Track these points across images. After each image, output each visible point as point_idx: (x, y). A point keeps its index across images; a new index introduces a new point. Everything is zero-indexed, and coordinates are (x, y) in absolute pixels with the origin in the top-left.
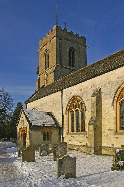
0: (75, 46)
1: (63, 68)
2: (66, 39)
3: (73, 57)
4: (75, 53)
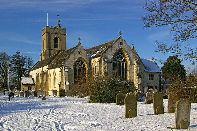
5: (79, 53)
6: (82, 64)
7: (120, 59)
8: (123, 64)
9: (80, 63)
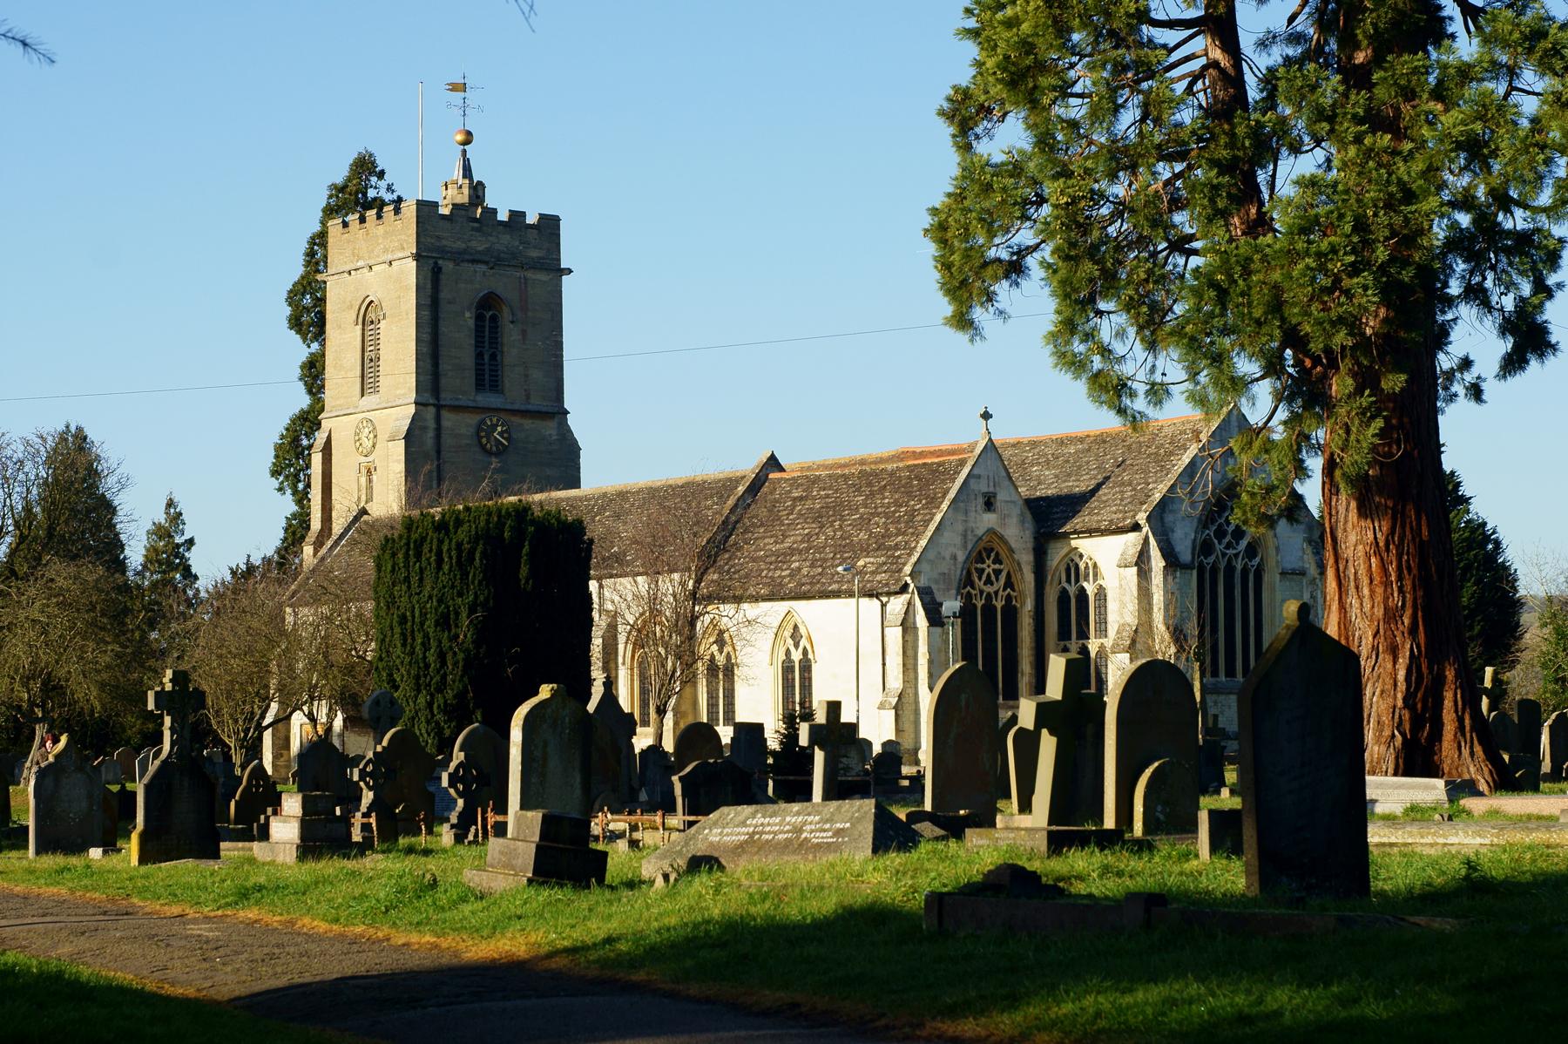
0: (503, 283)
1: (444, 413)
2: (460, 257)
3: (495, 341)
4: (506, 314)
5: (989, 505)
6: (997, 573)
7: (1228, 546)
8: (1245, 571)
9: (989, 567)
